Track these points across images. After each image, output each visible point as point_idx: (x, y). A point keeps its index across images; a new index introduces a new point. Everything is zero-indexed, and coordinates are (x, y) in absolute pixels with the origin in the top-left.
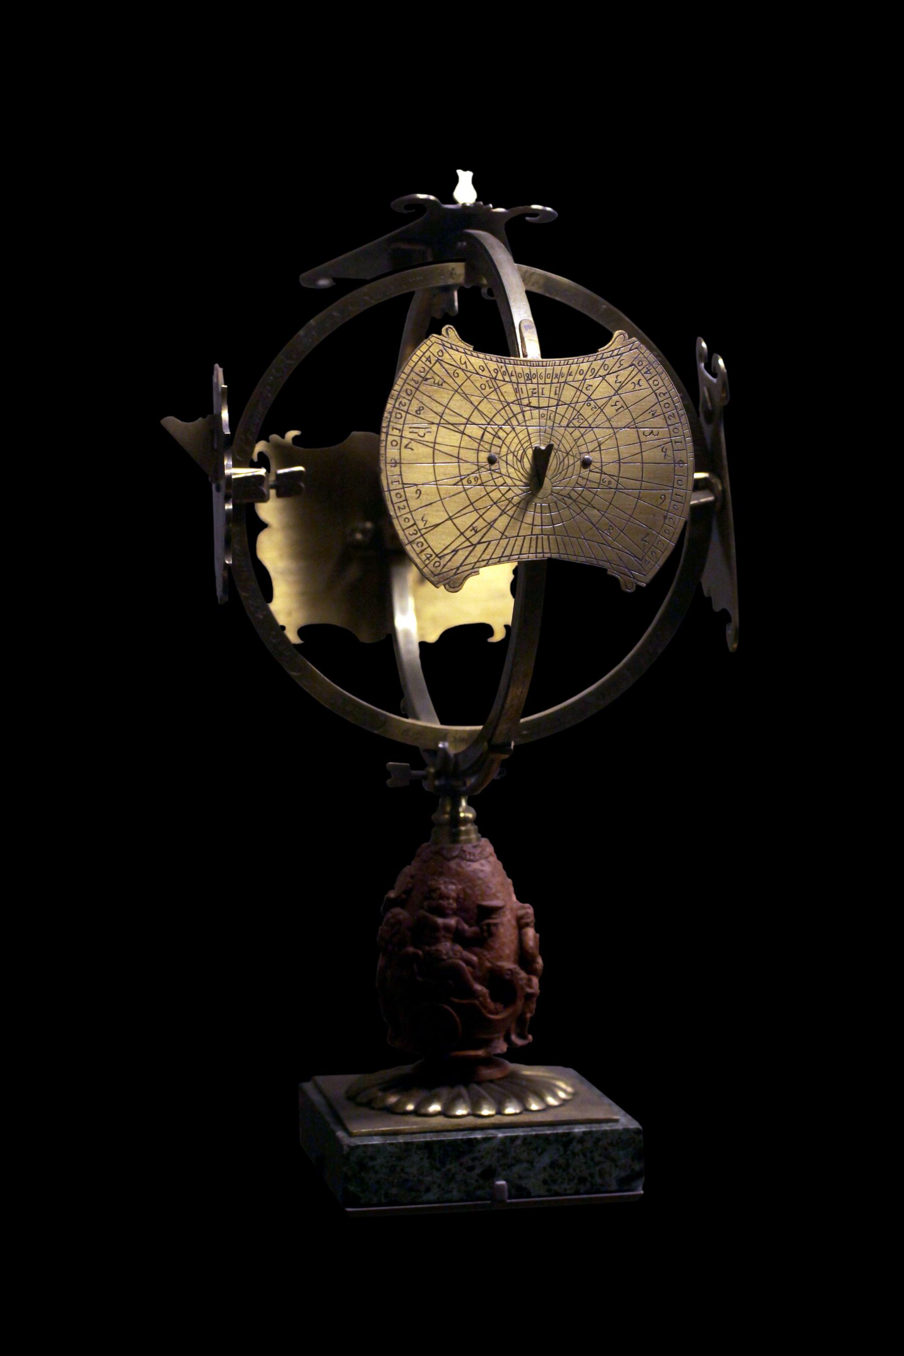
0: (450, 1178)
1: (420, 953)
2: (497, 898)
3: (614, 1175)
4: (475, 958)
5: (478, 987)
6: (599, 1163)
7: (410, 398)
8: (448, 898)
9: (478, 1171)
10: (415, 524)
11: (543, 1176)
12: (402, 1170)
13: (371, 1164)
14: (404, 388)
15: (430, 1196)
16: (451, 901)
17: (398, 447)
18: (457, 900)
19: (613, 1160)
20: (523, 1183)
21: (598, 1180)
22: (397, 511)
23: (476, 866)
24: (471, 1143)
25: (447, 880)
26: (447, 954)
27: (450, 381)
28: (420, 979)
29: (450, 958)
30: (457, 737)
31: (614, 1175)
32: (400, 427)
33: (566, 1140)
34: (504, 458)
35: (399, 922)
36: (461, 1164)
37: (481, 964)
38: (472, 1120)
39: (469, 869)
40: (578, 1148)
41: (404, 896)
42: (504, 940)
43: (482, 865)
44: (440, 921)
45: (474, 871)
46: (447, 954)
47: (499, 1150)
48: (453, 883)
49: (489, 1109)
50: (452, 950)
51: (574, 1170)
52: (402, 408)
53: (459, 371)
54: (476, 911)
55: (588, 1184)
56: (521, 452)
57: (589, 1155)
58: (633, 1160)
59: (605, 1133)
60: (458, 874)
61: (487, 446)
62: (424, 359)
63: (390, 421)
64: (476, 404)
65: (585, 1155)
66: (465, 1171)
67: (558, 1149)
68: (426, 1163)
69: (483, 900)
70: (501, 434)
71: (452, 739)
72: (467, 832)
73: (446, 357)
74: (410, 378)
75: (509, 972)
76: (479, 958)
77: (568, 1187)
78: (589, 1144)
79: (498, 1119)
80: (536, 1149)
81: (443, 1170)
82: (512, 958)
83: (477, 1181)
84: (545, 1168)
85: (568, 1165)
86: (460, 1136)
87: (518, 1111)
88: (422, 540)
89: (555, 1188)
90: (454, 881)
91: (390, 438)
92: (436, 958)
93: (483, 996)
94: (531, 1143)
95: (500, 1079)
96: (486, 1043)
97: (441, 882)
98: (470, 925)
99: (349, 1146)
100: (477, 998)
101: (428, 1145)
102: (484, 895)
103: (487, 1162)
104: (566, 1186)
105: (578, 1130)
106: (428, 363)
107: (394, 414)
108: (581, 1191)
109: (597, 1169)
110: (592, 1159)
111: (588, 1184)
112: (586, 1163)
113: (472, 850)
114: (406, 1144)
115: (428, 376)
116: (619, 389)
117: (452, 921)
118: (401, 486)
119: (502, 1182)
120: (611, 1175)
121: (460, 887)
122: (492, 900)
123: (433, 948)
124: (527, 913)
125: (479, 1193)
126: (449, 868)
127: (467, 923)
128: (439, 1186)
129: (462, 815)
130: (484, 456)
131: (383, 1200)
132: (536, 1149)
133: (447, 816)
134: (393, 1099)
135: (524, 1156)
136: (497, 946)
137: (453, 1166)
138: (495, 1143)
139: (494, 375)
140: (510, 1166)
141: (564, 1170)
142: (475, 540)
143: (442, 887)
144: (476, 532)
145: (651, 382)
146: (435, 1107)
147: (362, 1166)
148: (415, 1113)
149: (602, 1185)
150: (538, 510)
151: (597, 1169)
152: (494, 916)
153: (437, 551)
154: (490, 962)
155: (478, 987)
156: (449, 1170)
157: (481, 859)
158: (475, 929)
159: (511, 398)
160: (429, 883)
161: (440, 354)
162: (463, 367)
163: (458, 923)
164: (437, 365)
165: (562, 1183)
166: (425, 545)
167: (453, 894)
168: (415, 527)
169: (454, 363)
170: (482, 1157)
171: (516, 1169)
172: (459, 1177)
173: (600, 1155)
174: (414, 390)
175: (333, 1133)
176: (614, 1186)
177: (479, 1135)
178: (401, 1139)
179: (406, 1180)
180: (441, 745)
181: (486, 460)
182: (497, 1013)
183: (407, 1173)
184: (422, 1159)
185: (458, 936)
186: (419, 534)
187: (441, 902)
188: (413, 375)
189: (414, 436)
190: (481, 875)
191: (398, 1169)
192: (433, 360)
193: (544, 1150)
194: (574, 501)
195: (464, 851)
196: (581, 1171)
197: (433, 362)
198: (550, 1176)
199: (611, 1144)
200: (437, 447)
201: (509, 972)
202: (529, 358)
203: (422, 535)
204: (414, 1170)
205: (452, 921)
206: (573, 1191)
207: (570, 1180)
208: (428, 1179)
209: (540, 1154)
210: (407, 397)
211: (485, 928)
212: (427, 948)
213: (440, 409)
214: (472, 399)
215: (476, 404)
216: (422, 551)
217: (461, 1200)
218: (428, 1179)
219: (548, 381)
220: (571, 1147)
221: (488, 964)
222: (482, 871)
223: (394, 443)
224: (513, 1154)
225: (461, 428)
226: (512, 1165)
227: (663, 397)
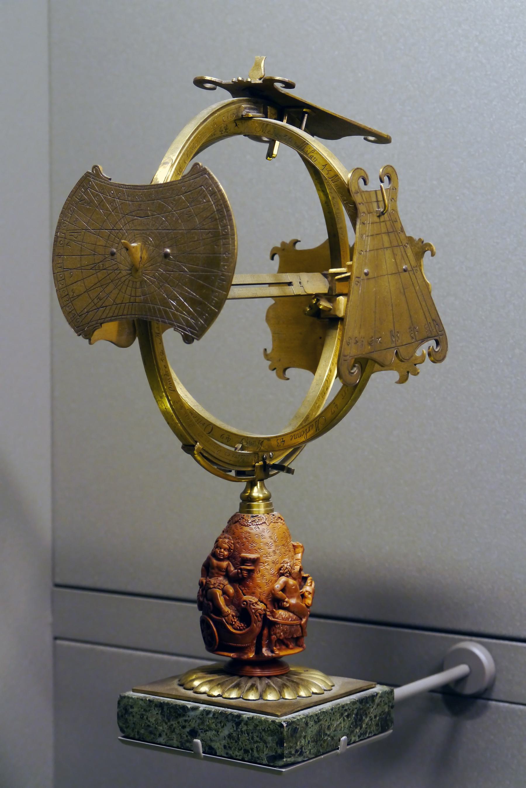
3: (265, 753)
6: (257, 742)
8: (221, 548)
9: (188, 729)
11: (224, 742)
12: (147, 718)
13: (131, 710)
15: (161, 740)
16: (222, 550)
19: (265, 743)
20: (212, 744)
21: (256, 754)
31: (265, 753)
33: (237, 721)
36: (178, 723)
40: (245, 728)
48: (229, 538)
57: (250, 734)
58: (277, 743)
65: (248, 734)
68: (160, 717)
72: (258, 506)
75: (245, 603)
77: (238, 754)
80: (221, 722)
83: (187, 736)
94: (217, 718)
96: (242, 650)
100: (224, 617)
101: (161, 705)
103: (193, 724)
104: (236, 753)
112: (248, 740)
114: (150, 701)
127: (234, 566)
128: (166, 734)
131: (137, 737)
132: (221, 722)
135: (213, 726)
137: (174, 723)
138: (197, 713)
144: (100, 300)
149: (258, 758)
155: (226, 609)
156: (172, 725)
163: (228, 565)
165: (235, 750)
168: (68, 296)
171: (209, 733)
172: (177, 731)
173: (257, 737)
176: (265, 761)
177: (190, 704)
179: (149, 726)
182: (240, 630)
183: (149, 721)
184: (157, 714)
191: (145, 717)
194: (112, 281)
196: (246, 745)
199: (264, 730)
203: (71, 302)
204: (152, 720)
205: (225, 564)
207: (240, 750)
209: (223, 727)
217: (177, 747)
218: (161, 728)
220: (240, 727)
226: (207, 731)
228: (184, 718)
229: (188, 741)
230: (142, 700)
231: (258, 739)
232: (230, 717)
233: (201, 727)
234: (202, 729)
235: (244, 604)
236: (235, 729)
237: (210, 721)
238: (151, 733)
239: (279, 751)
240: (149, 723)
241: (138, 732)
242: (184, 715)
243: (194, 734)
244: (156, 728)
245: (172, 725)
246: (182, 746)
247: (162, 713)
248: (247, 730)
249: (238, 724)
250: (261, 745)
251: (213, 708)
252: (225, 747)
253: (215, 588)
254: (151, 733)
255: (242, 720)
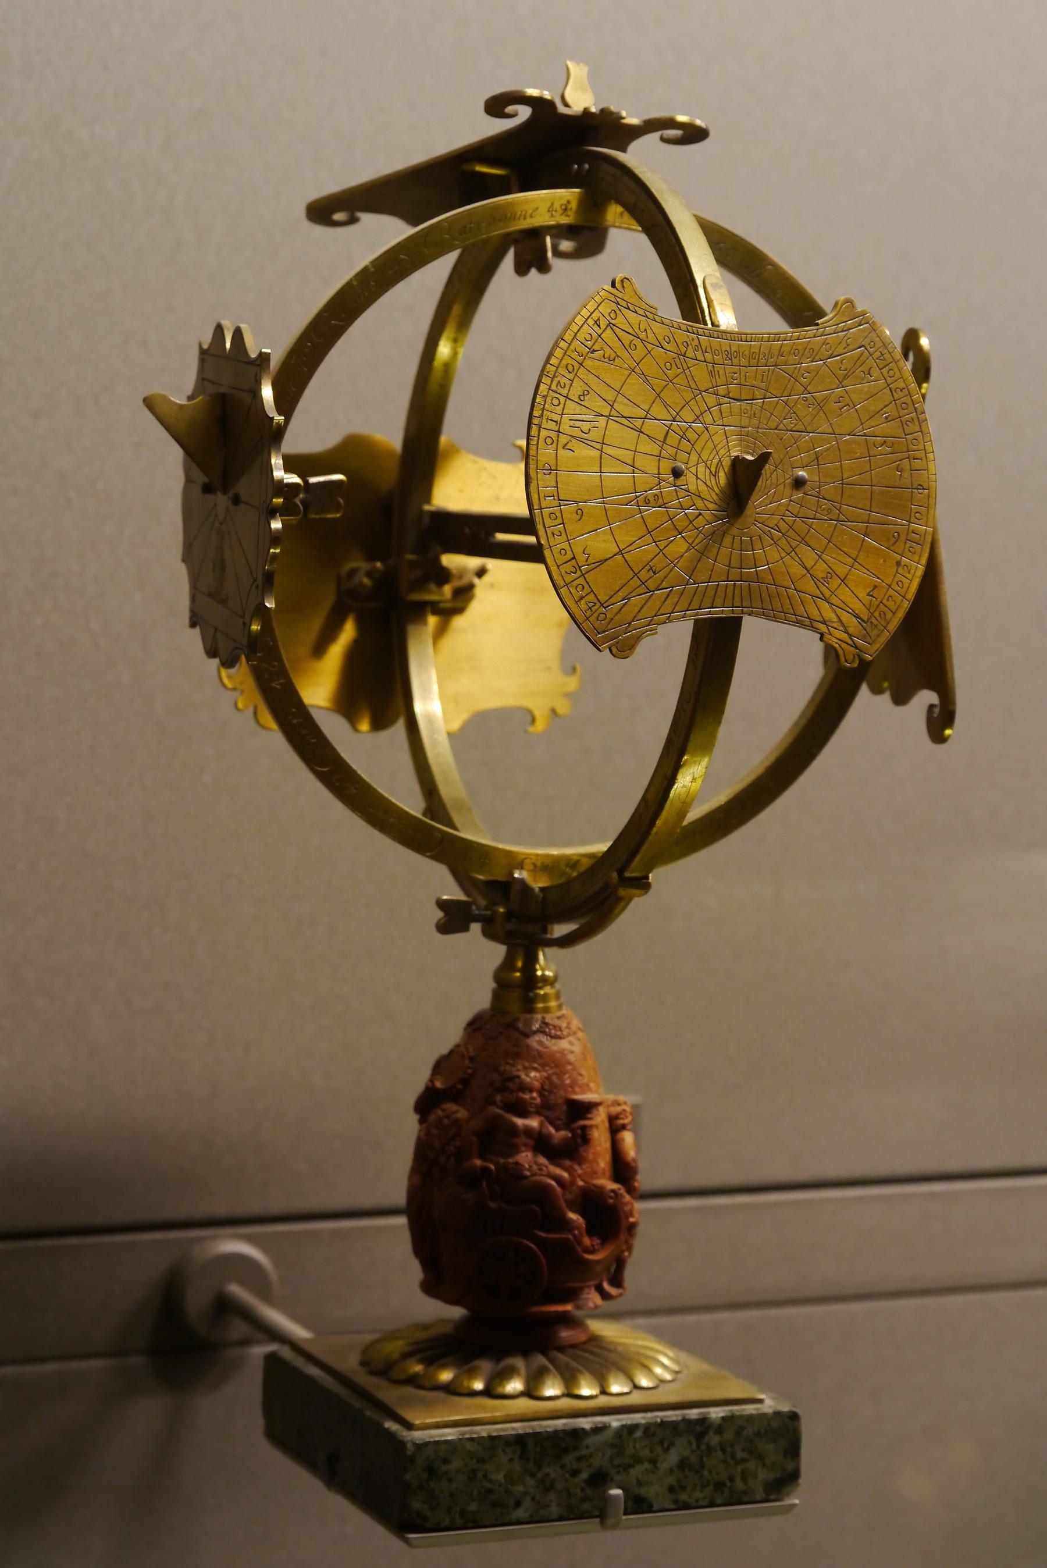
0: (548, 1486)
1: (492, 1167)
2: (590, 1090)
4: (565, 1175)
5: (572, 1216)
6: (744, 1460)
7: (571, 376)
8: (531, 1090)
9: (584, 1475)
10: (574, 558)
11: (671, 1480)
12: (485, 1476)
13: (444, 1468)
14: (564, 362)
15: (520, 1513)
16: (535, 1094)
17: (554, 445)
18: (542, 1091)
19: (760, 1457)
20: (643, 1491)
22: (551, 539)
23: (564, 1044)
24: (577, 1434)
25: (527, 1064)
26: (530, 1168)
27: (624, 354)
28: (492, 1205)
29: (533, 1175)
30: (539, 864)
32: (556, 418)
34: (693, 470)
35: (457, 1123)
36: (562, 1467)
37: (573, 1182)
38: (567, 1403)
39: (555, 1048)
41: (459, 1086)
42: (598, 1148)
43: (571, 1043)
44: (520, 1122)
45: (562, 1052)
46: (530, 1168)
47: (613, 1445)
49: (589, 1387)
50: (536, 1163)
51: (710, 1472)
52: (560, 390)
53: (637, 341)
54: (564, 1108)
55: (727, 1492)
56: (716, 461)
57: (729, 1449)
59: (750, 1418)
60: (540, 1055)
61: (672, 451)
62: (591, 322)
63: (543, 409)
64: (658, 390)
65: (723, 1450)
66: (567, 1475)
67: (690, 1443)
68: (517, 1466)
69: (575, 1093)
70: (691, 435)
71: (531, 867)
73: (620, 321)
74: (572, 347)
75: (612, 1194)
76: (570, 1174)
78: (729, 1435)
79: (603, 1401)
80: (662, 1442)
81: (539, 1475)
82: (608, 1174)
83: (583, 1490)
84: (671, 1470)
85: (702, 1466)
86: (560, 1423)
87: (626, 1390)
88: (581, 581)
89: (684, 1497)
90: (536, 1065)
91: (544, 433)
92: (516, 1174)
93: (578, 1228)
94: (654, 1435)
95: (584, 1343)
97: (520, 1067)
98: (557, 1129)
99: (415, 1444)
101: (520, 1441)
102: (574, 1084)
103: (597, 1462)
104: (698, 1494)
105: (716, 1413)
106: (596, 328)
107: (549, 400)
108: (718, 1501)
109: (739, 1469)
110: (733, 1456)
111: (727, 1492)
112: (724, 1462)
113: (557, 1022)
114: (491, 1438)
115: (595, 348)
116: (845, 379)
117: (534, 1123)
118: (556, 503)
119: (619, 1492)
120: (756, 1477)
121: (545, 1074)
122: (584, 1093)
123: (511, 1160)
124: (624, 1110)
125: (585, 1506)
126: (528, 1047)
128: (533, 1499)
129: (539, 973)
130: (666, 466)
133: (518, 974)
134: (446, 1376)
135: (645, 1453)
136: (591, 1157)
137: (552, 1471)
138: (607, 1436)
139: (683, 349)
140: (627, 1467)
141: (697, 1472)
142: (651, 584)
143: (523, 1076)
145: (885, 371)
146: (515, 1385)
147: (431, 1471)
148: (488, 1393)
149: (745, 1493)
150: (737, 545)
151: (739, 1469)
152: (589, 1116)
153: (603, 599)
154: (583, 1180)
155: (572, 1216)
156: (548, 1475)
157: (569, 1035)
158: (563, 1134)
159: (704, 382)
160: (502, 1068)
161: (613, 315)
162: (643, 335)
163: (541, 1124)
164: (609, 331)
166: (587, 590)
167: (537, 1084)
169: (630, 330)
170: (591, 1456)
171: (636, 1472)
172: (560, 1485)
173: (743, 1450)
174: (576, 366)
175: (379, 1426)
176: (760, 1494)
177: (585, 1423)
178: (483, 1431)
179: (489, 1491)
180: (516, 875)
181: (669, 472)
183: (491, 1481)
184: (511, 1460)
185: (541, 1144)
186: (579, 573)
187: (521, 1095)
188: (576, 343)
189: (576, 432)
190: (571, 1058)
191: (480, 1475)
192: (603, 323)
193: (672, 1444)
195: (547, 1024)
196: (718, 1474)
197: (603, 327)
198: (679, 1481)
199: (758, 1434)
200: (606, 449)
201: (612, 1194)
202: (723, 327)
204: (500, 1477)
205: (534, 1123)
206: (705, 1503)
207: (704, 1487)
208: (520, 1488)
209: (668, 1449)
210: (567, 375)
211: (579, 1131)
212: (502, 1161)
213: (610, 396)
214: (653, 381)
215: (658, 390)
216: (582, 598)
218: (520, 1488)
219: (754, 362)
220: (706, 1440)
221: (581, 1183)
222: (572, 1052)
223: (549, 441)
224: (630, 1451)
225: (638, 423)
226: (631, 1466)
227: (901, 394)
228: (577, 1454)
229: (584, 1500)
230: (472, 1439)
231: (745, 1455)
232: (682, 1426)
233: (616, 1462)
234: (619, 1466)
235: (611, 1198)
236: (694, 1447)
237: (638, 1446)
238: (495, 1504)
239: (790, 1467)
240: (488, 1485)
241: (462, 1512)
242: (576, 1448)
243: (600, 1480)
244: (507, 1491)
245: (548, 1475)
246: (572, 1513)
247: (524, 1456)
248: (720, 1443)
249: (700, 1436)
250: (751, 1465)
251: (638, 1418)
252: (671, 1489)
253: (533, 1175)
254: (495, 1504)
255: (710, 1426)
